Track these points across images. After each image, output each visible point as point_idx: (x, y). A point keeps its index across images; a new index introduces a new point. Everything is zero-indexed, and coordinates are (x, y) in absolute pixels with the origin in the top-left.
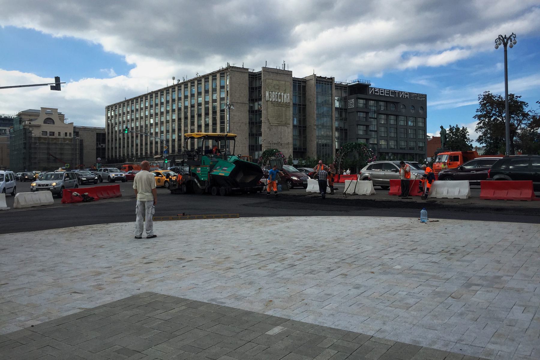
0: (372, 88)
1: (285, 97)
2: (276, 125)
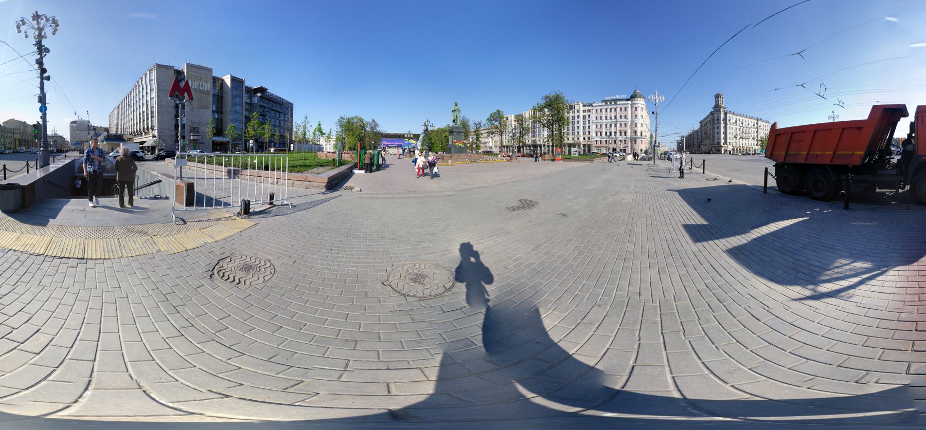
1: (206, 86)
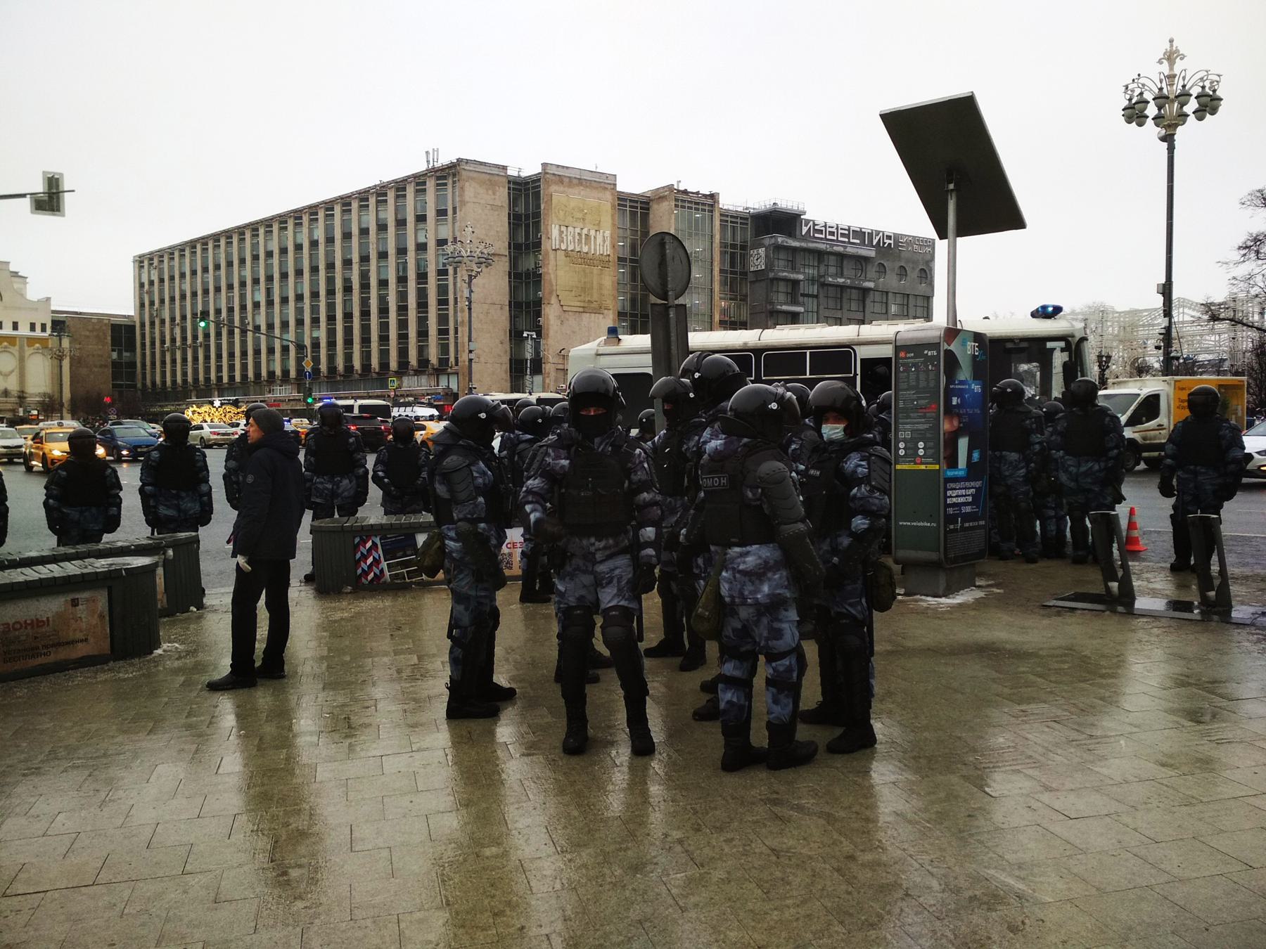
0: (807, 222)
1: (599, 240)
2: (575, 309)
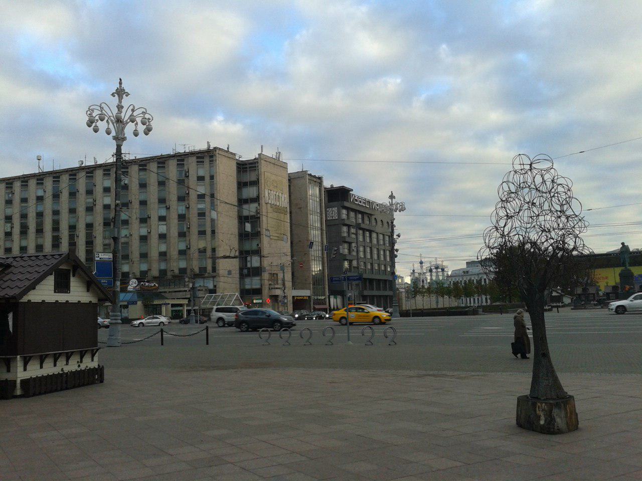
0: (353, 195)
1: (283, 198)
